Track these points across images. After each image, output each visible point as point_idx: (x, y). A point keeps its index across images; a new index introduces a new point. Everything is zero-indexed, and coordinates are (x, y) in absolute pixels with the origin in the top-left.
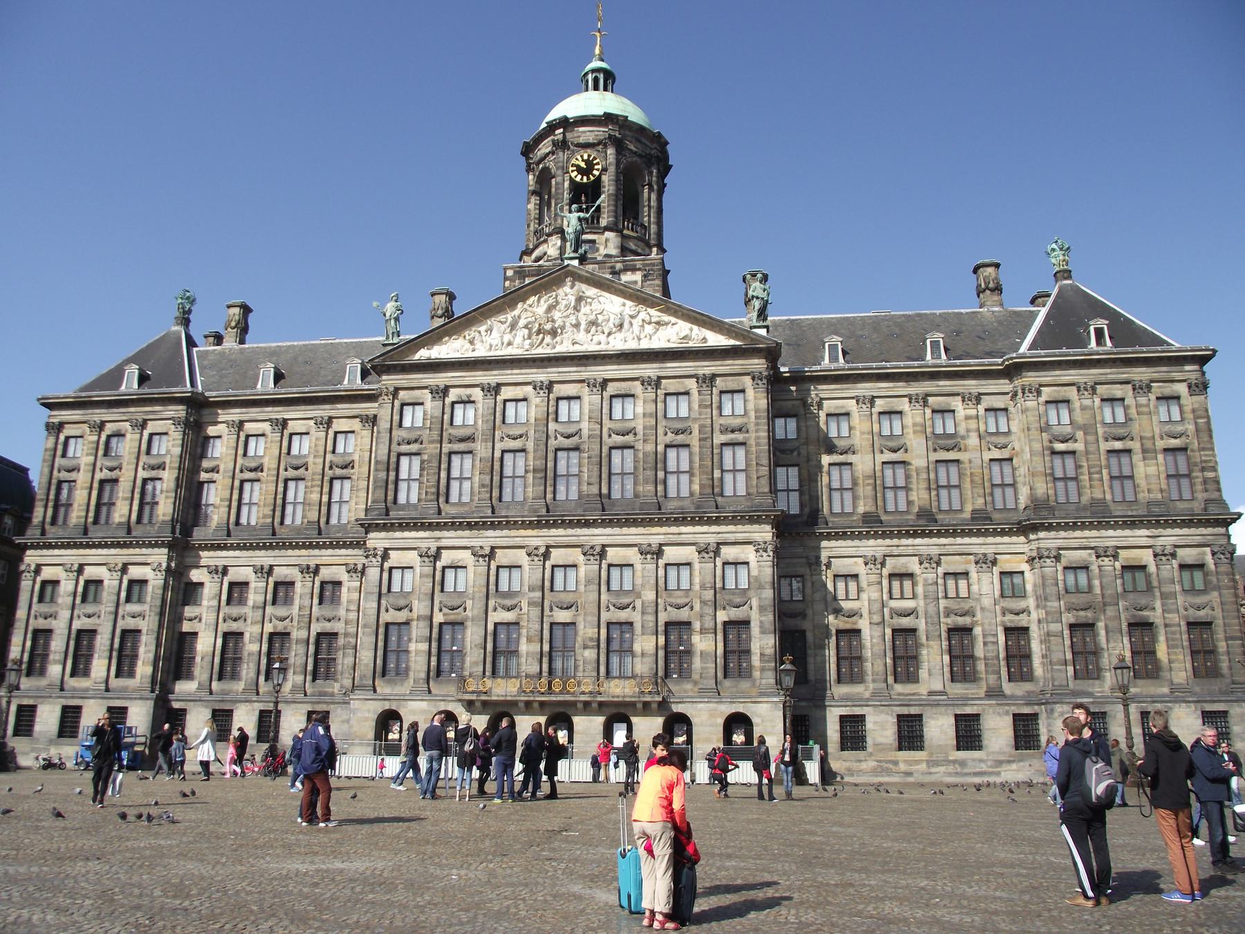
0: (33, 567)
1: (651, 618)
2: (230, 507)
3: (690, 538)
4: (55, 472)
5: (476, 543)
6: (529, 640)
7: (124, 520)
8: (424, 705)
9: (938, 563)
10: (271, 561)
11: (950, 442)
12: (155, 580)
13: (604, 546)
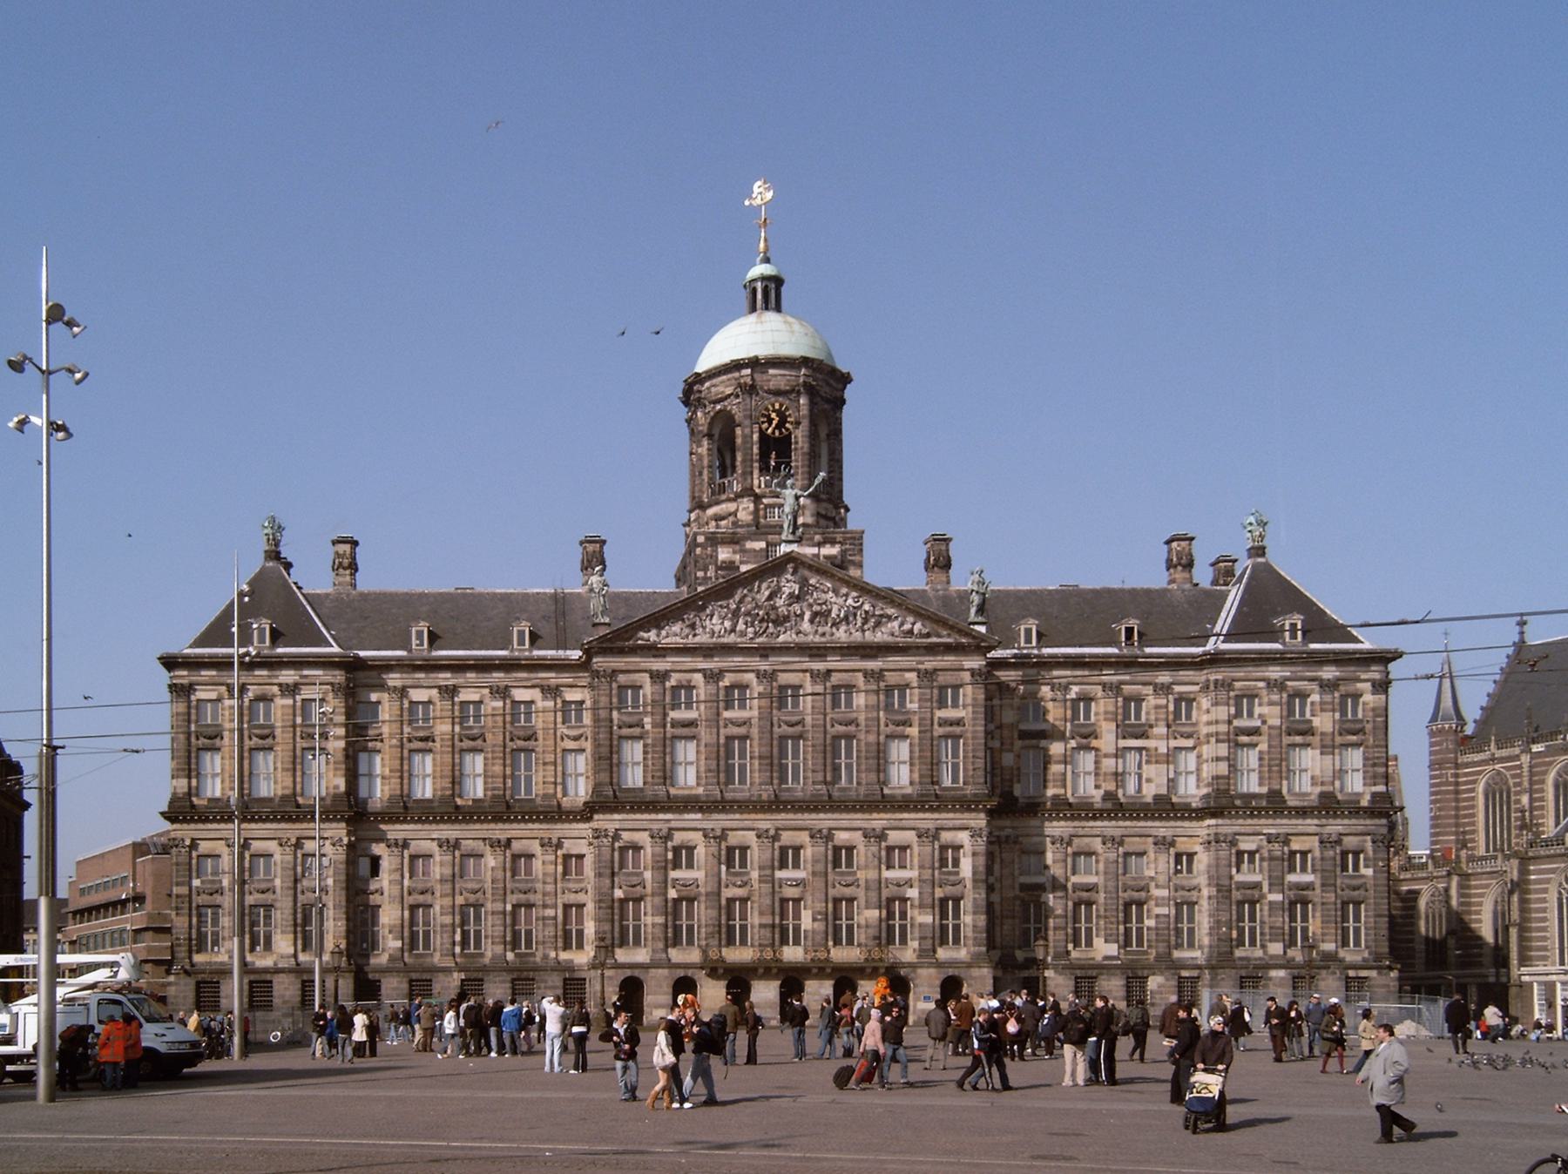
0: (188, 842)
1: (873, 895)
2: (401, 778)
4: (193, 739)
5: (708, 825)
6: (761, 914)
7: (287, 792)
8: (666, 972)
9: (1121, 843)
11: (1137, 730)
12: (334, 854)
13: (830, 829)
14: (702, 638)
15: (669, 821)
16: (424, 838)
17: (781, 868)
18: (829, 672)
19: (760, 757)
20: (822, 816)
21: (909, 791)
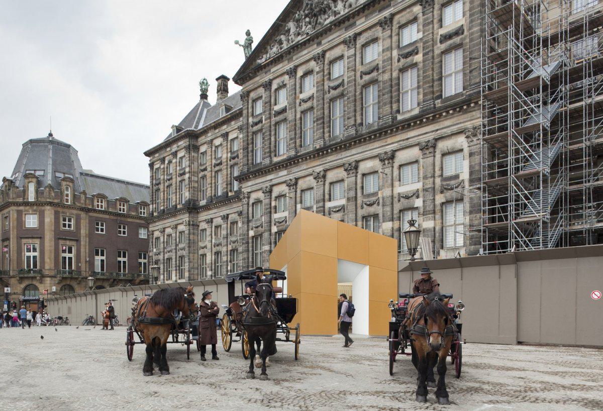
1: (388, 209)
3: (416, 140)
5: (287, 178)
10: (228, 212)
13: (357, 162)
14: (285, 46)
15: (271, 180)
16: (216, 214)
17: (330, 200)
18: (357, 35)
19: (317, 120)
20: (354, 151)
21: (416, 112)
